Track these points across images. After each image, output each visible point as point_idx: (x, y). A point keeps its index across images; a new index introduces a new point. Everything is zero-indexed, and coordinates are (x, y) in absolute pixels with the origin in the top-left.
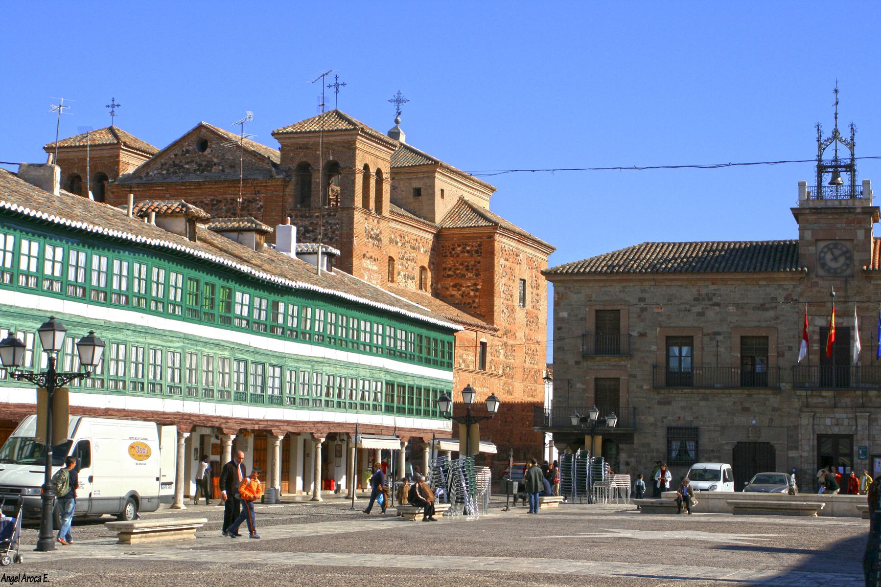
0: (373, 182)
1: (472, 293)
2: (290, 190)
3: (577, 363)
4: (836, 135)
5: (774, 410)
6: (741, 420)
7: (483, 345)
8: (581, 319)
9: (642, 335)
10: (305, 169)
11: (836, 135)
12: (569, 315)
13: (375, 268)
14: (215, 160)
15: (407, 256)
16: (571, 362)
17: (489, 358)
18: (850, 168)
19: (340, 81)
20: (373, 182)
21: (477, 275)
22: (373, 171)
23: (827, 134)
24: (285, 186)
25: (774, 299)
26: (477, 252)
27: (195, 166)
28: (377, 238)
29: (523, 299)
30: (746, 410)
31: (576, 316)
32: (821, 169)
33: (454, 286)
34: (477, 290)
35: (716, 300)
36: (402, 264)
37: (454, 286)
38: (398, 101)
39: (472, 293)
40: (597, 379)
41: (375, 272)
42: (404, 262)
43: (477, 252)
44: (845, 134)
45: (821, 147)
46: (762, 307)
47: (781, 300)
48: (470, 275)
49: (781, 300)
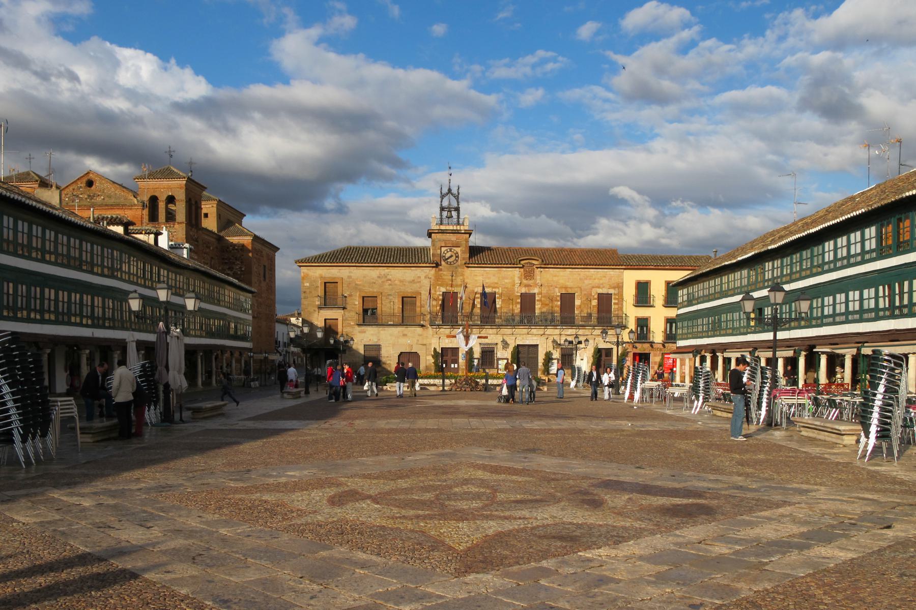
4: (450, 190)
5: (420, 335)
6: (403, 341)
9: (350, 295)
10: (154, 200)
11: (450, 190)
18: (457, 209)
20: (193, 208)
22: (193, 202)
23: (445, 190)
25: (419, 277)
29: (264, 277)
30: (405, 335)
32: (442, 209)
35: (389, 277)
37: (229, 269)
44: (454, 191)
45: (443, 197)
46: (413, 281)
47: (423, 278)
49: (423, 278)
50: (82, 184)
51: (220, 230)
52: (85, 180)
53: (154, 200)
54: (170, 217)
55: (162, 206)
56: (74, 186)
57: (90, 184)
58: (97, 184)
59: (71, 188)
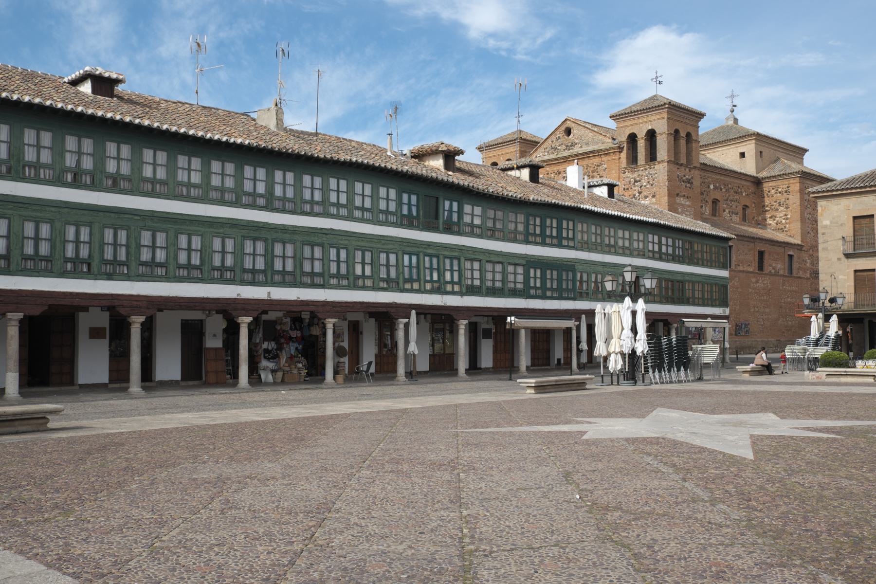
0: (683, 142)
1: (784, 221)
2: (624, 155)
3: (839, 259)
7: (791, 256)
8: (841, 225)
10: (632, 138)
12: (831, 222)
13: (687, 203)
14: (577, 141)
15: (731, 198)
16: (835, 259)
17: (795, 265)
19: (659, 75)
21: (787, 208)
22: (683, 134)
24: (620, 152)
26: (786, 192)
27: (564, 147)
28: (689, 181)
31: (837, 223)
33: (771, 217)
34: (787, 219)
36: (727, 204)
38: (732, 96)
39: (784, 221)
40: (856, 271)
41: (688, 206)
42: (729, 202)
43: (786, 192)
48: (782, 208)
50: (560, 133)
51: (759, 169)
52: (563, 128)
53: (632, 138)
54: (652, 156)
55: (641, 144)
56: (553, 138)
57: (568, 132)
58: (574, 131)
59: (549, 141)
